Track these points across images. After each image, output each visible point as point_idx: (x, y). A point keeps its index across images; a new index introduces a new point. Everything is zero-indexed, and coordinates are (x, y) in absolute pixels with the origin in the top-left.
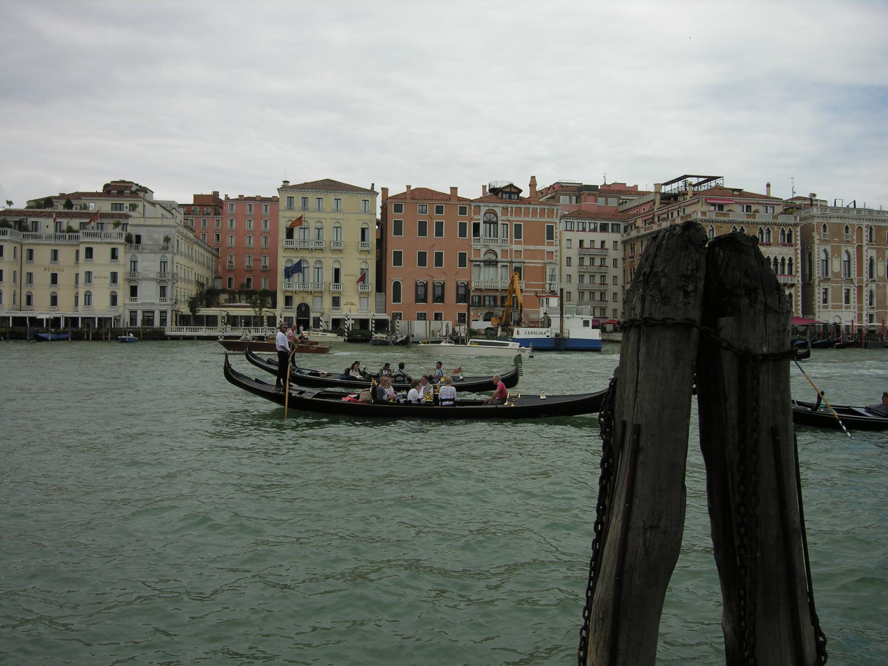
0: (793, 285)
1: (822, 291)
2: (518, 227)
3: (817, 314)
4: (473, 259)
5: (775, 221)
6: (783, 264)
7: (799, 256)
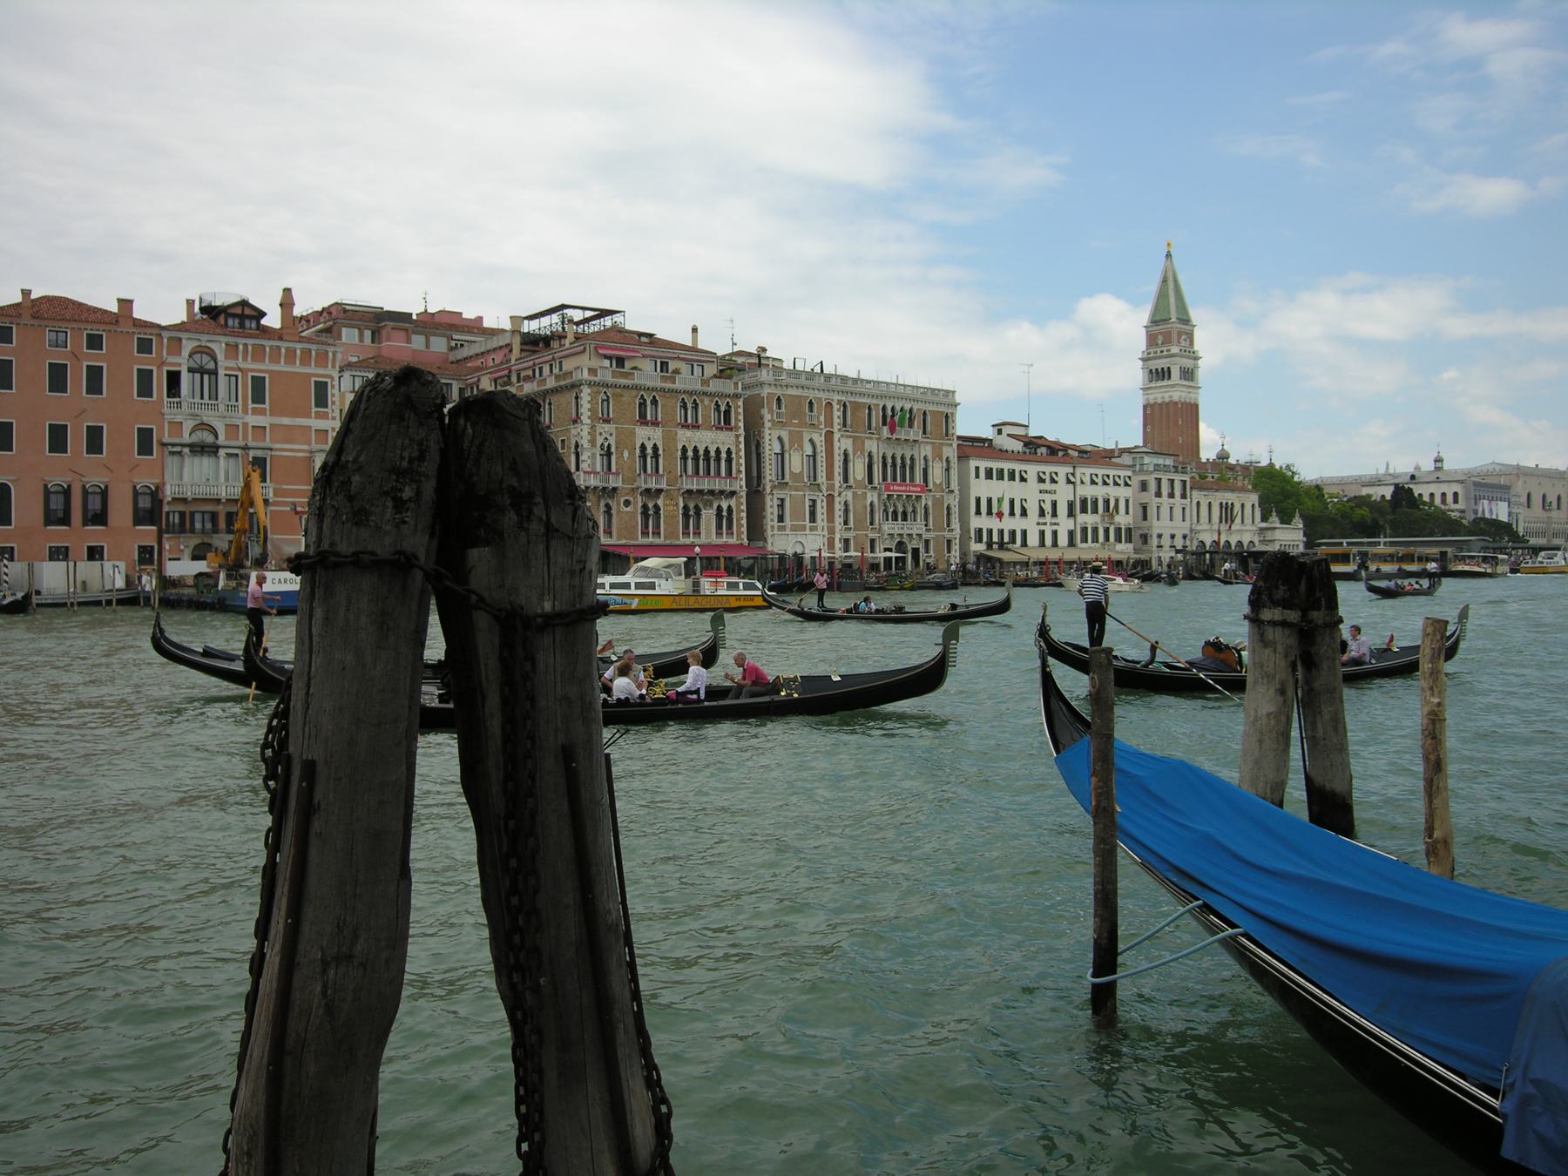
0: (733, 493)
1: (776, 502)
2: (258, 383)
3: (770, 540)
4: (166, 439)
5: (705, 389)
6: (718, 459)
7: (742, 446)
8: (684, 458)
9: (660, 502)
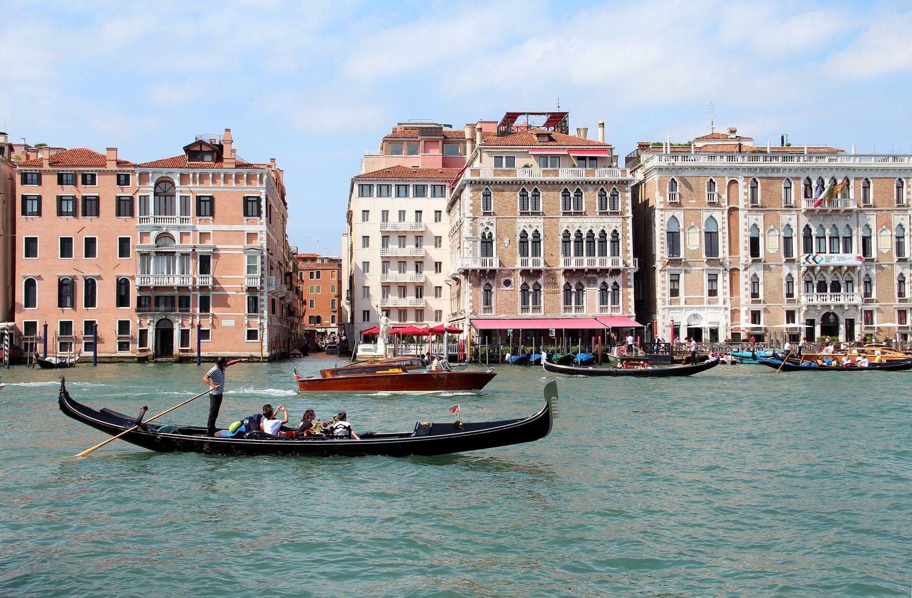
0: (616, 272)
5: (591, 178)
7: (630, 228)
8: (566, 241)
9: (541, 281)
